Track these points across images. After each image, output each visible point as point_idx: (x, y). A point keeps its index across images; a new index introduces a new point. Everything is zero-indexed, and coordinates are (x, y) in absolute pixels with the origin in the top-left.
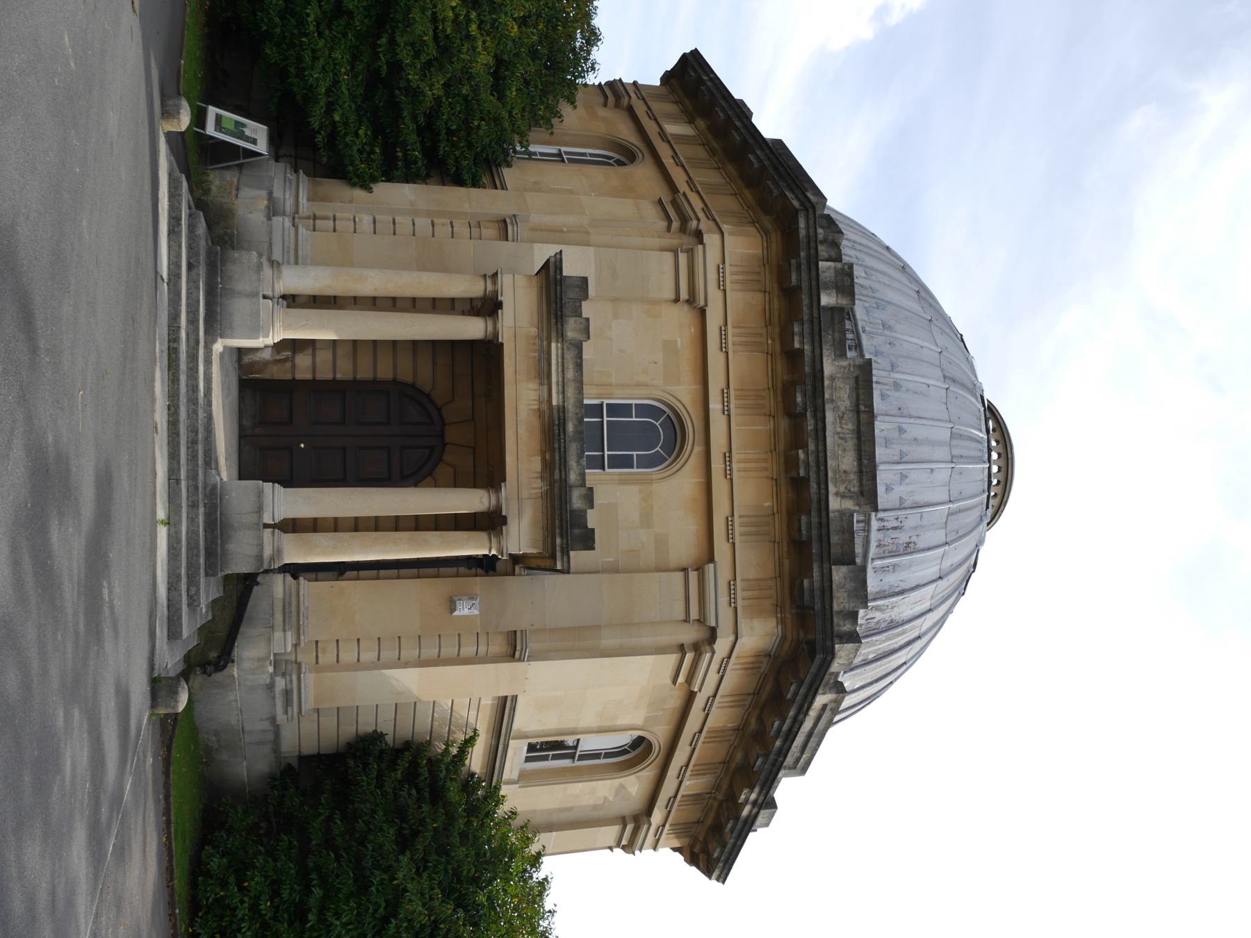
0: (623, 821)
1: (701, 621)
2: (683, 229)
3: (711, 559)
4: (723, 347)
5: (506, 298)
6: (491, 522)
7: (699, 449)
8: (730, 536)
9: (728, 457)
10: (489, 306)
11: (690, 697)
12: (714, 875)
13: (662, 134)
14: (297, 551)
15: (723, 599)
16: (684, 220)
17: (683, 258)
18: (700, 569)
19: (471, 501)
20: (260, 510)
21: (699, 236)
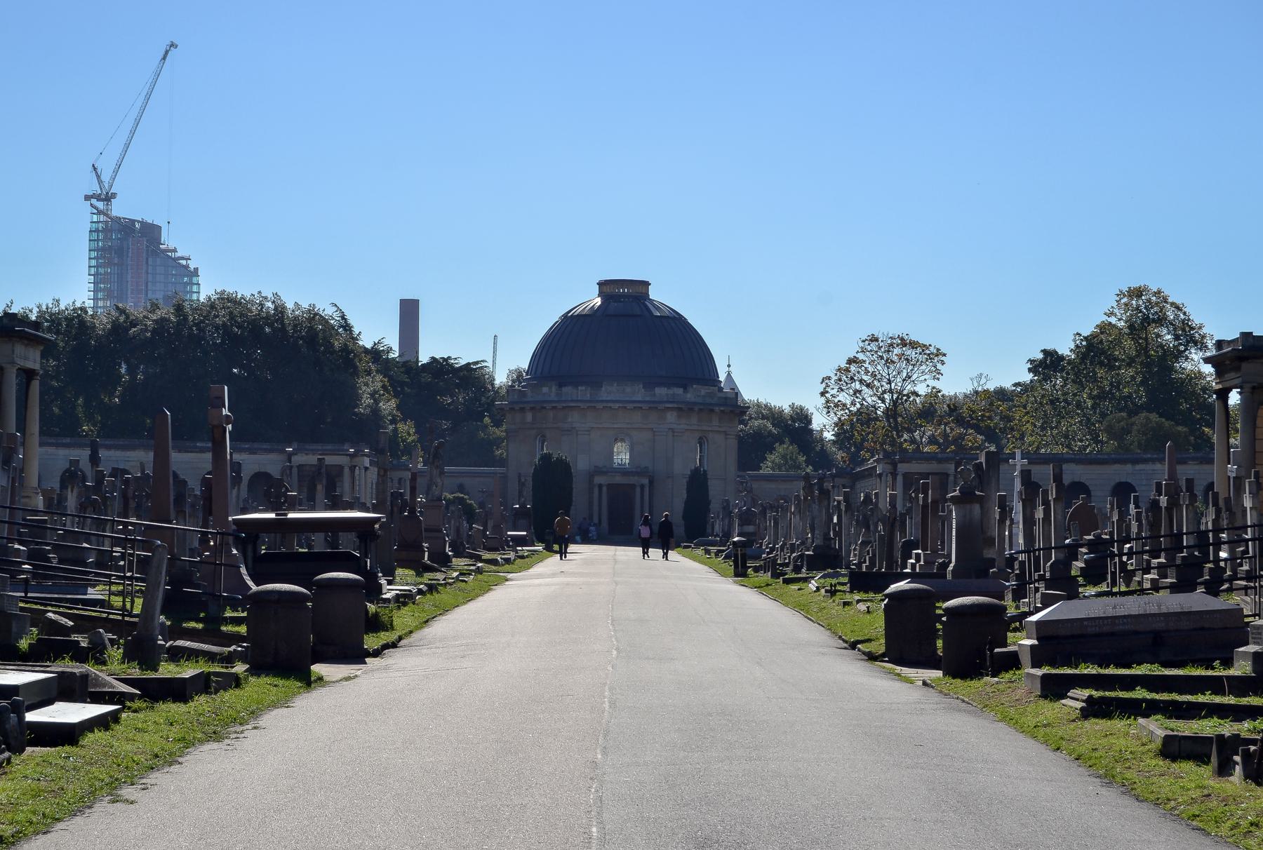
10: (600, 486)
19: (638, 490)
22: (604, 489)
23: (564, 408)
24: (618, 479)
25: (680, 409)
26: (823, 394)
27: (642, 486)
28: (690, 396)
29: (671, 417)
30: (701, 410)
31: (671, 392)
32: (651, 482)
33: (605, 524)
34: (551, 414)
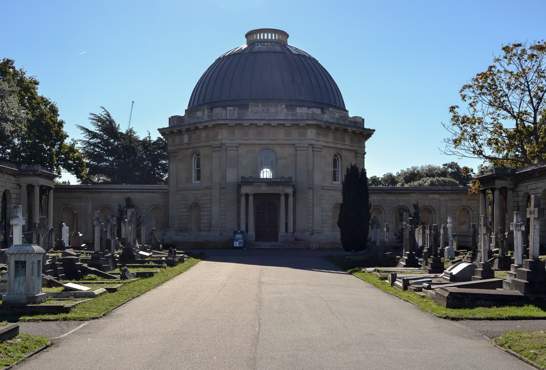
0: (356, 156)
1: (308, 147)
2: (220, 147)
4: (248, 140)
6: (287, 196)
7: (270, 146)
8: (289, 140)
9: (272, 140)
10: (247, 196)
13: (189, 144)
14: (291, 229)
15: (303, 142)
16: (218, 147)
17: (228, 148)
18: (296, 147)
19: (283, 199)
20: (284, 236)
21: (222, 144)
22: (251, 198)
23: (215, 126)
24: (264, 189)
25: (318, 127)
26: (452, 109)
27: (287, 196)
28: (326, 117)
29: (311, 134)
30: (336, 129)
31: (310, 111)
32: (294, 193)
33: (252, 232)
34: (203, 134)
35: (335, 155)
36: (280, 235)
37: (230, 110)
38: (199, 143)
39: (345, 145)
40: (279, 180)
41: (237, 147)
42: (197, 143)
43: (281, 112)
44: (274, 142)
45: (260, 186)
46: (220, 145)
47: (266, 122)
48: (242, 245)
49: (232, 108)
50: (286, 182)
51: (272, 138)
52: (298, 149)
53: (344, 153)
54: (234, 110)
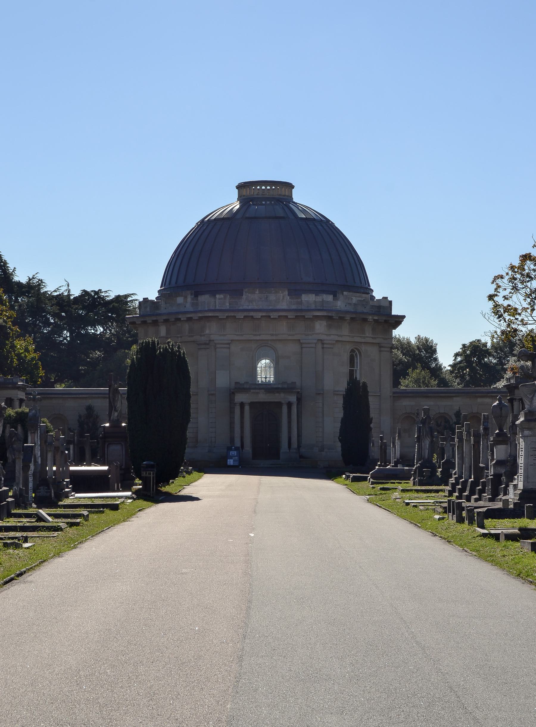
0: (380, 351)
2: (208, 344)
3: (299, 340)
5: (241, 401)
6: (290, 405)
9: (272, 335)
10: (242, 405)
11: (337, 341)
12: (401, 320)
14: (295, 445)
16: (205, 344)
17: (218, 346)
18: (302, 344)
19: (285, 409)
21: (210, 340)
22: (247, 408)
23: (201, 318)
24: (262, 397)
25: (330, 318)
26: (491, 297)
27: (290, 405)
28: (340, 304)
29: (320, 327)
30: (352, 319)
31: (319, 299)
32: (299, 400)
33: (248, 448)
34: (186, 326)
35: (353, 351)
36: (281, 451)
37: (219, 299)
38: (181, 337)
39: (364, 338)
40: (280, 386)
41: (229, 344)
42: (178, 337)
43: (282, 300)
44: (274, 338)
45: (258, 393)
46: (207, 342)
47: (264, 314)
48: (237, 464)
49: (222, 296)
50: (289, 388)
51: (272, 333)
52: (304, 345)
53: (363, 348)
54: (225, 298)
